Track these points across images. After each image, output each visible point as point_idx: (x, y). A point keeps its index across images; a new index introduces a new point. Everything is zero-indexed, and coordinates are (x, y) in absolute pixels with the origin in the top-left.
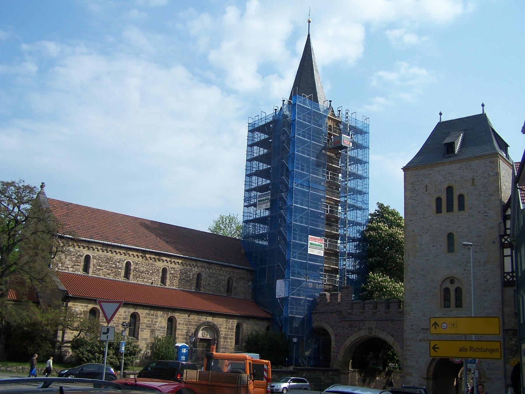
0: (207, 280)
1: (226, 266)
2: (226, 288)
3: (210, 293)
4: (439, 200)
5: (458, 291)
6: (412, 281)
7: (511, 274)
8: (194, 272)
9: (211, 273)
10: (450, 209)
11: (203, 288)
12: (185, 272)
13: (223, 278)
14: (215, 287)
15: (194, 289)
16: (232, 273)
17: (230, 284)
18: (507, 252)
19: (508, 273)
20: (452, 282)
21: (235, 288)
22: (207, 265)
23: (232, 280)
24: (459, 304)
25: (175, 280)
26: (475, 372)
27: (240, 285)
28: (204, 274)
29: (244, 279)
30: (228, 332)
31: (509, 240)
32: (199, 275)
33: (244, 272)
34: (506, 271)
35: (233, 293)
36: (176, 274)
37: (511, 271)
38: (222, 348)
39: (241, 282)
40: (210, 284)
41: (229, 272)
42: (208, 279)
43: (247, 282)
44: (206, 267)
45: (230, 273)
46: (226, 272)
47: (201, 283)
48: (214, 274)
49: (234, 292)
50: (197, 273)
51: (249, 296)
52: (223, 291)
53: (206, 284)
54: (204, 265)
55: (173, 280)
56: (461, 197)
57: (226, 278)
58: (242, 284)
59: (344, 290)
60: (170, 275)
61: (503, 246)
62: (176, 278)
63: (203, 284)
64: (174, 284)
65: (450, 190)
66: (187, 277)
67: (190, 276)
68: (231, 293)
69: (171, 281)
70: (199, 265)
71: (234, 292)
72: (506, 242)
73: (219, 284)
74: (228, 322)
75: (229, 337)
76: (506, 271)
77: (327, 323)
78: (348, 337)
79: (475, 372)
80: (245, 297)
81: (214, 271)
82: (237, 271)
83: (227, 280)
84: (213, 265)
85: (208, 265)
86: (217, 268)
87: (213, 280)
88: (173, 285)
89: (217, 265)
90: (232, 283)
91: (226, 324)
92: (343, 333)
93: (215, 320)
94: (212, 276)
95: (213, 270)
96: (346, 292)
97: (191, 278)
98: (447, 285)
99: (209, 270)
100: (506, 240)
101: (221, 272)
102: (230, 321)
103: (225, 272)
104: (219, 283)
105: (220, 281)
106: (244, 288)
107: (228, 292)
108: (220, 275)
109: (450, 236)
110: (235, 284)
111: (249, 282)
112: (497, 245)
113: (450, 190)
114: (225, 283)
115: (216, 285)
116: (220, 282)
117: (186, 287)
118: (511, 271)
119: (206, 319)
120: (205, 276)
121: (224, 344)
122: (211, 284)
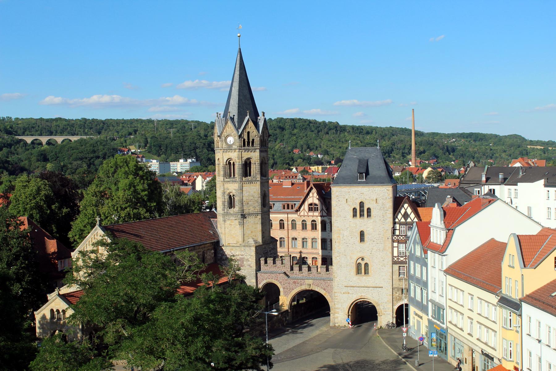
4: (355, 210)
5: (366, 265)
6: (338, 258)
7: (397, 257)
10: (362, 215)
18: (395, 244)
19: (396, 257)
20: (363, 259)
24: (366, 272)
31: (397, 238)
34: (394, 255)
37: (397, 255)
56: (369, 210)
61: (393, 241)
65: (362, 204)
72: (395, 239)
76: (394, 255)
77: (277, 280)
78: (293, 289)
92: (289, 287)
98: (360, 261)
100: (395, 238)
109: (362, 234)
112: (390, 240)
113: (362, 204)
118: (397, 255)
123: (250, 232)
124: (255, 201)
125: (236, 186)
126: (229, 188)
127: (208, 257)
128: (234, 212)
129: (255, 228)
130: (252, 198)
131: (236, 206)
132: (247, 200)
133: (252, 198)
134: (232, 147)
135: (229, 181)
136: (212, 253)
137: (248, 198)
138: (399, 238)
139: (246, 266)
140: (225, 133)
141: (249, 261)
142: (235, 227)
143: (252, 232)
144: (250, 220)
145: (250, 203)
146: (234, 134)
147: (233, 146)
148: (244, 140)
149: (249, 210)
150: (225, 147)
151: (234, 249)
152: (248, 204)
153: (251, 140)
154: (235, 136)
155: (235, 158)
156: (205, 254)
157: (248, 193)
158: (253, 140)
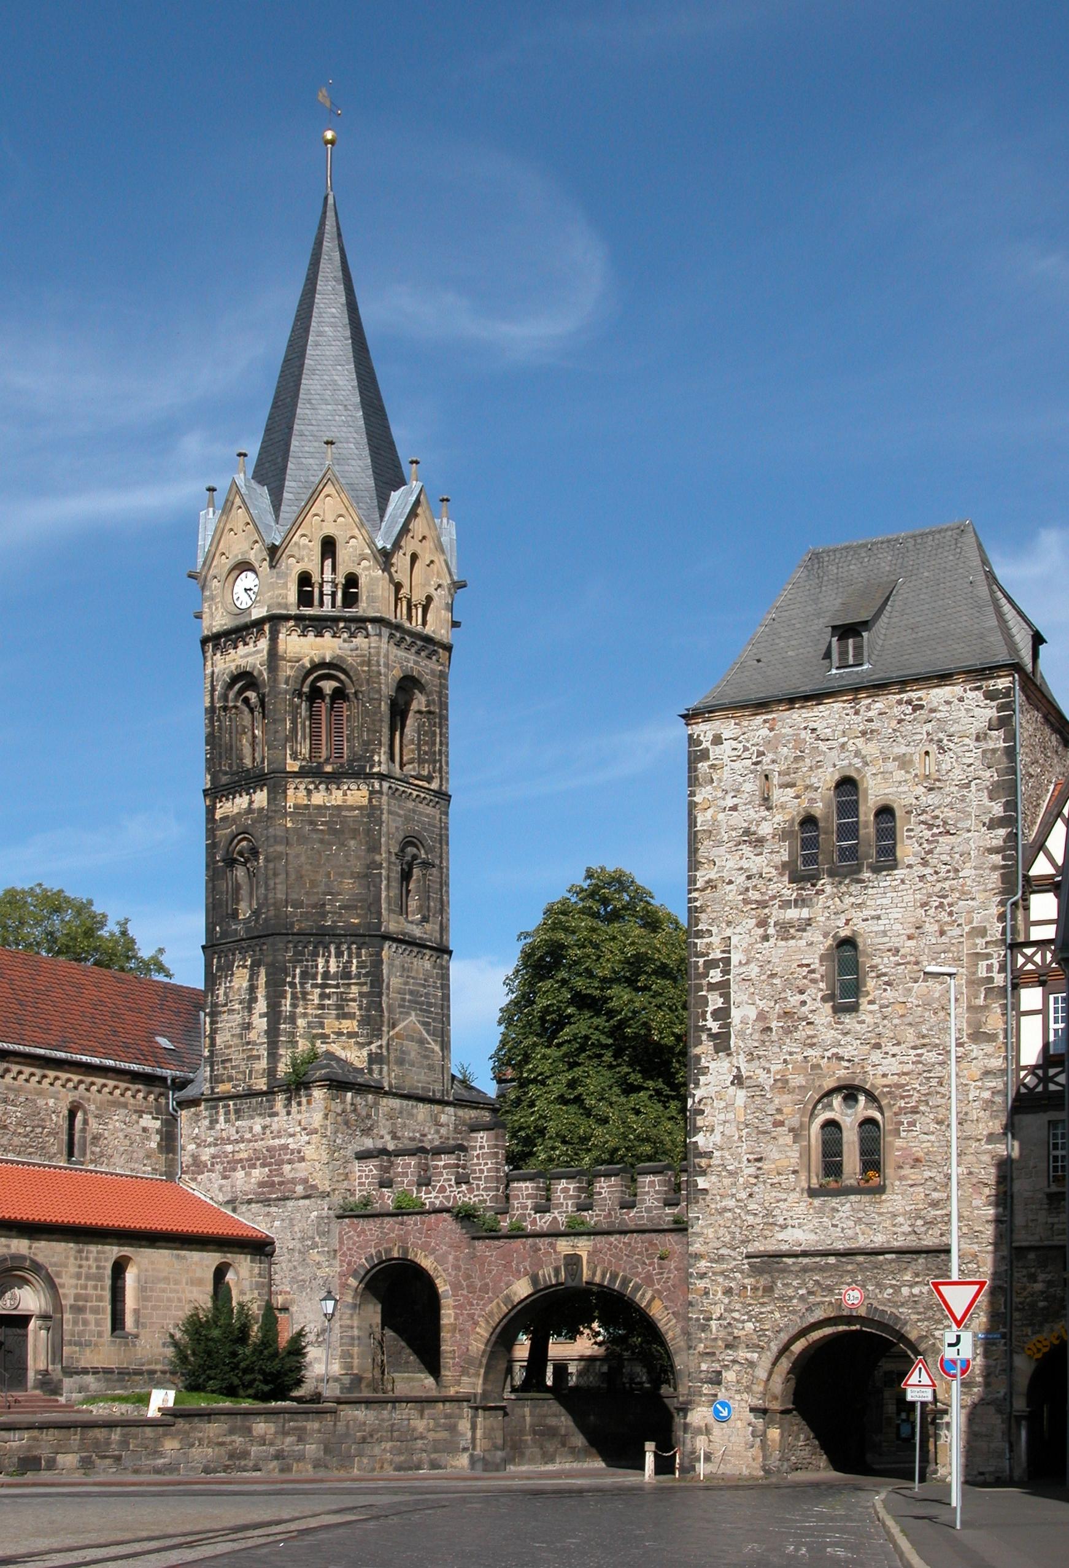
21: (96, 1138)
26: (958, 1337)
27: (110, 1127)
30: (85, 1287)
38: (70, 1343)
39: (116, 1117)
51: (145, 1165)
58: (117, 1124)
59: (481, 1134)
71: (93, 1153)
74: (84, 1255)
75: (89, 1304)
79: (958, 1337)
80: (132, 1170)
91: (78, 1262)
93: (36, 1248)
96: (485, 1144)
102: (91, 1252)
110: (95, 1125)
111: (141, 1117)
119: (8, 1246)
121: (76, 1329)
136: (145, 1130)
138: (1038, 959)
141: (302, 1159)
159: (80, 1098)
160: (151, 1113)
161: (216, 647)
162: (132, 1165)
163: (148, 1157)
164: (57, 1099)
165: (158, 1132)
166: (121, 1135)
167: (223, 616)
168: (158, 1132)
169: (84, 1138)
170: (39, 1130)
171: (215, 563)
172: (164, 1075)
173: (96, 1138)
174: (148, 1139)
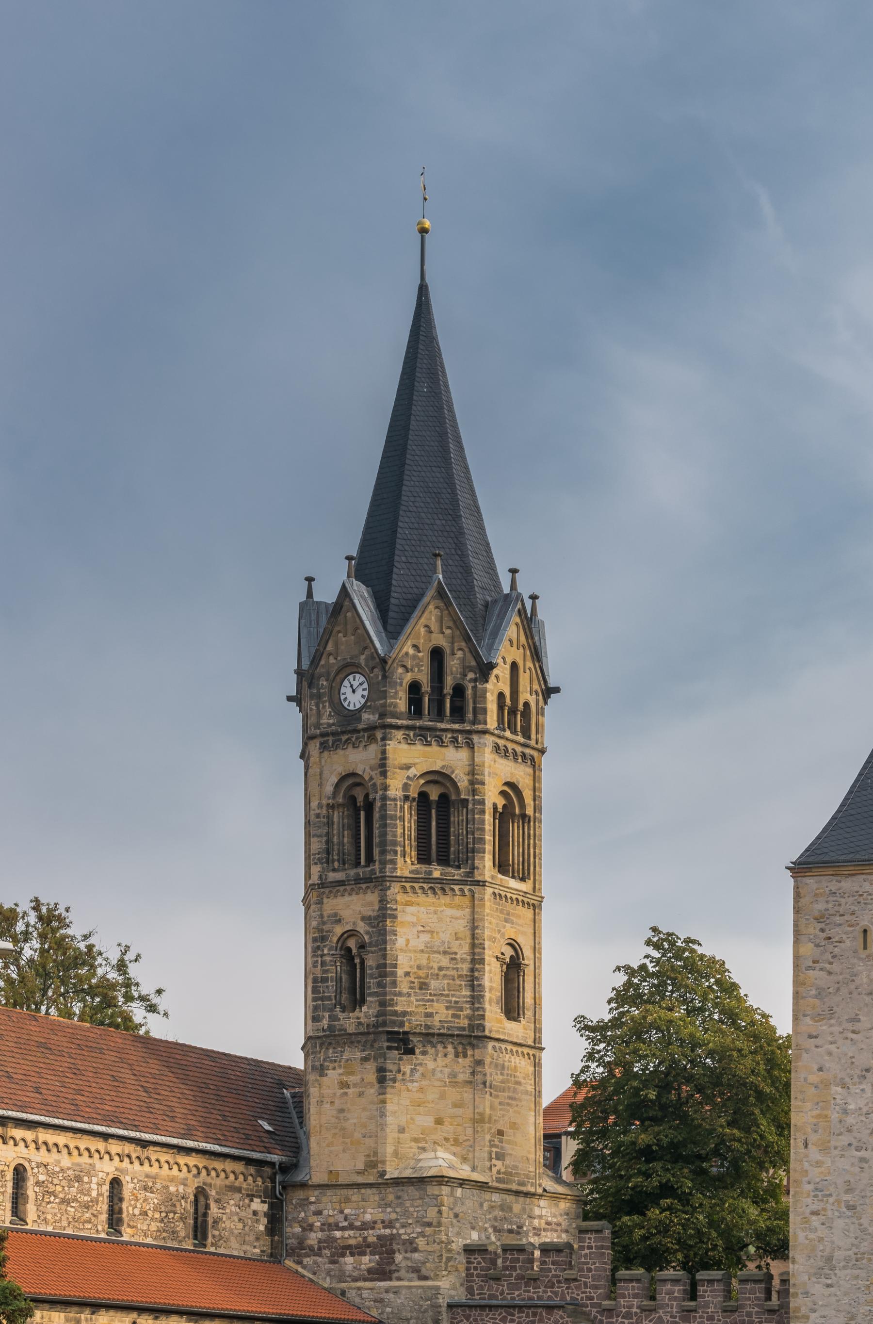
0: (137, 1200)
1: (188, 1151)
2: (192, 1222)
3: (149, 1240)
8: (101, 1175)
9: (147, 1176)
11: (129, 1226)
12: (76, 1177)
13: (181, 1189)
14: (162, 1221)
15: (103, 1230)
16: (204, 1172)
17: (201, 1210)
22: (135, 1151)
23: (207, 1197)
25: (48, 1203)
27: (228, 1211)
28: (128, 1178)
29: (239, 1190)
32: (116, 1183)
33: (239, 1167)
35: (210, 1240)
36: (52, 1183)
39: (232, 1202)
40: (146, 1214)
41: (194, 1171)
42: (142, 1195)
43: (247, 1201)
44: (134, 1156)
45: (199, 1173)
46: (189, 1172)
47: (120, 1211)
48: (154, 1178)
49: (214, 1236)
50: (111, 1177)
51: (255, 1247)
52: (182, 1234)
53: (137, 1212)
54: (126, 1152)
55: (44, 1204)
57: (191, 1191)
58: (233, 1208)
60: (37, 1189)
62: (52, 1198)
63: (128, 1211)
64: (49, 1217)
66: (81, 1192)
67: (89, 1190)
68: (205, 1237)
69: (41, 1208)
70: (113, 1152)
71: (214, 1236)
73: (171, 1212)
81: (155, 1169)
82: (219, 1165)
83: (192, 1198)
84: (151, 1148)
85: (138, 1148)
86: (164, 1157)
87: (154, 1199)
88: (45, 1219)
89: (164, 1150)
90: (207, 1207)
94: (150, 1184)
95: (151, 1166)
97: (94, 1194)
99: (141, 1164)
101: (175, 1171)
103: (185, 1169)
104: (170, 1208)
105: (175, 1198)
106: (240, 1219)
107: (195, 1238)
108: (172, 1180)
111: (252, 1201)
114: (188, 1206)
115: (164, 1214)
116: (174, 1205)
117: (81, 1227)
120: (131, 1186)
122: (150, 1213)
123: (428, 1121)
124: (460, 976)
125: (371, 904)
126: (345, 914)
127: (228, 1224)
128: (360, 1023)
129: (455, 1105)
130: (445, 961)
131: (370, 995)
132: (419, 967)
133: (445, 961)
134: (359, 720)
135: (341, 883)
136: (255, 1213)
137: (424, 962)
139: (402, 1273)
140: (332, 660)
142: (361, 1094)
143: (439, 1122)
144: (431, 1065)
145: (433, 984)
146: (366, 660)
147: (365, 716)
148: (414, 688)
149: (429, 1015)
150: (330, 725)
151: (354, 1198)
152: (424, 986)
153: (448, 689)
154: (371, 664)
155: (372, 769)
156: (213, 1205)
157: (425, 937)
158: (459, 691)
159: (204, 1183)
160: (260, 1197)
161: (324, 747)
162: (245, 1247)
163: (257, 1239)
164: (185, 1185)
165: (266, 1215)
166: (236, 1218)
167: (330, 715)
168: (266, 1215)
169: (205, 1222)
170: (171, 1215)
171: (322, 662)
172: (273, 1160)
173: (216, 1222)
174: (258, 1221)
